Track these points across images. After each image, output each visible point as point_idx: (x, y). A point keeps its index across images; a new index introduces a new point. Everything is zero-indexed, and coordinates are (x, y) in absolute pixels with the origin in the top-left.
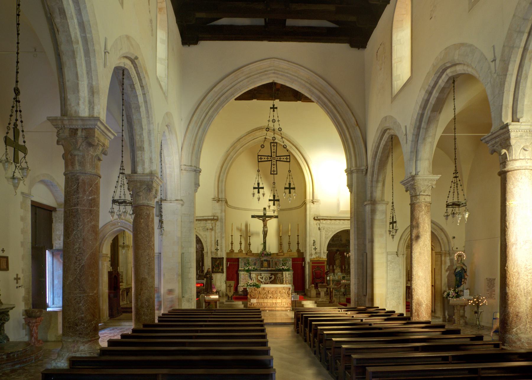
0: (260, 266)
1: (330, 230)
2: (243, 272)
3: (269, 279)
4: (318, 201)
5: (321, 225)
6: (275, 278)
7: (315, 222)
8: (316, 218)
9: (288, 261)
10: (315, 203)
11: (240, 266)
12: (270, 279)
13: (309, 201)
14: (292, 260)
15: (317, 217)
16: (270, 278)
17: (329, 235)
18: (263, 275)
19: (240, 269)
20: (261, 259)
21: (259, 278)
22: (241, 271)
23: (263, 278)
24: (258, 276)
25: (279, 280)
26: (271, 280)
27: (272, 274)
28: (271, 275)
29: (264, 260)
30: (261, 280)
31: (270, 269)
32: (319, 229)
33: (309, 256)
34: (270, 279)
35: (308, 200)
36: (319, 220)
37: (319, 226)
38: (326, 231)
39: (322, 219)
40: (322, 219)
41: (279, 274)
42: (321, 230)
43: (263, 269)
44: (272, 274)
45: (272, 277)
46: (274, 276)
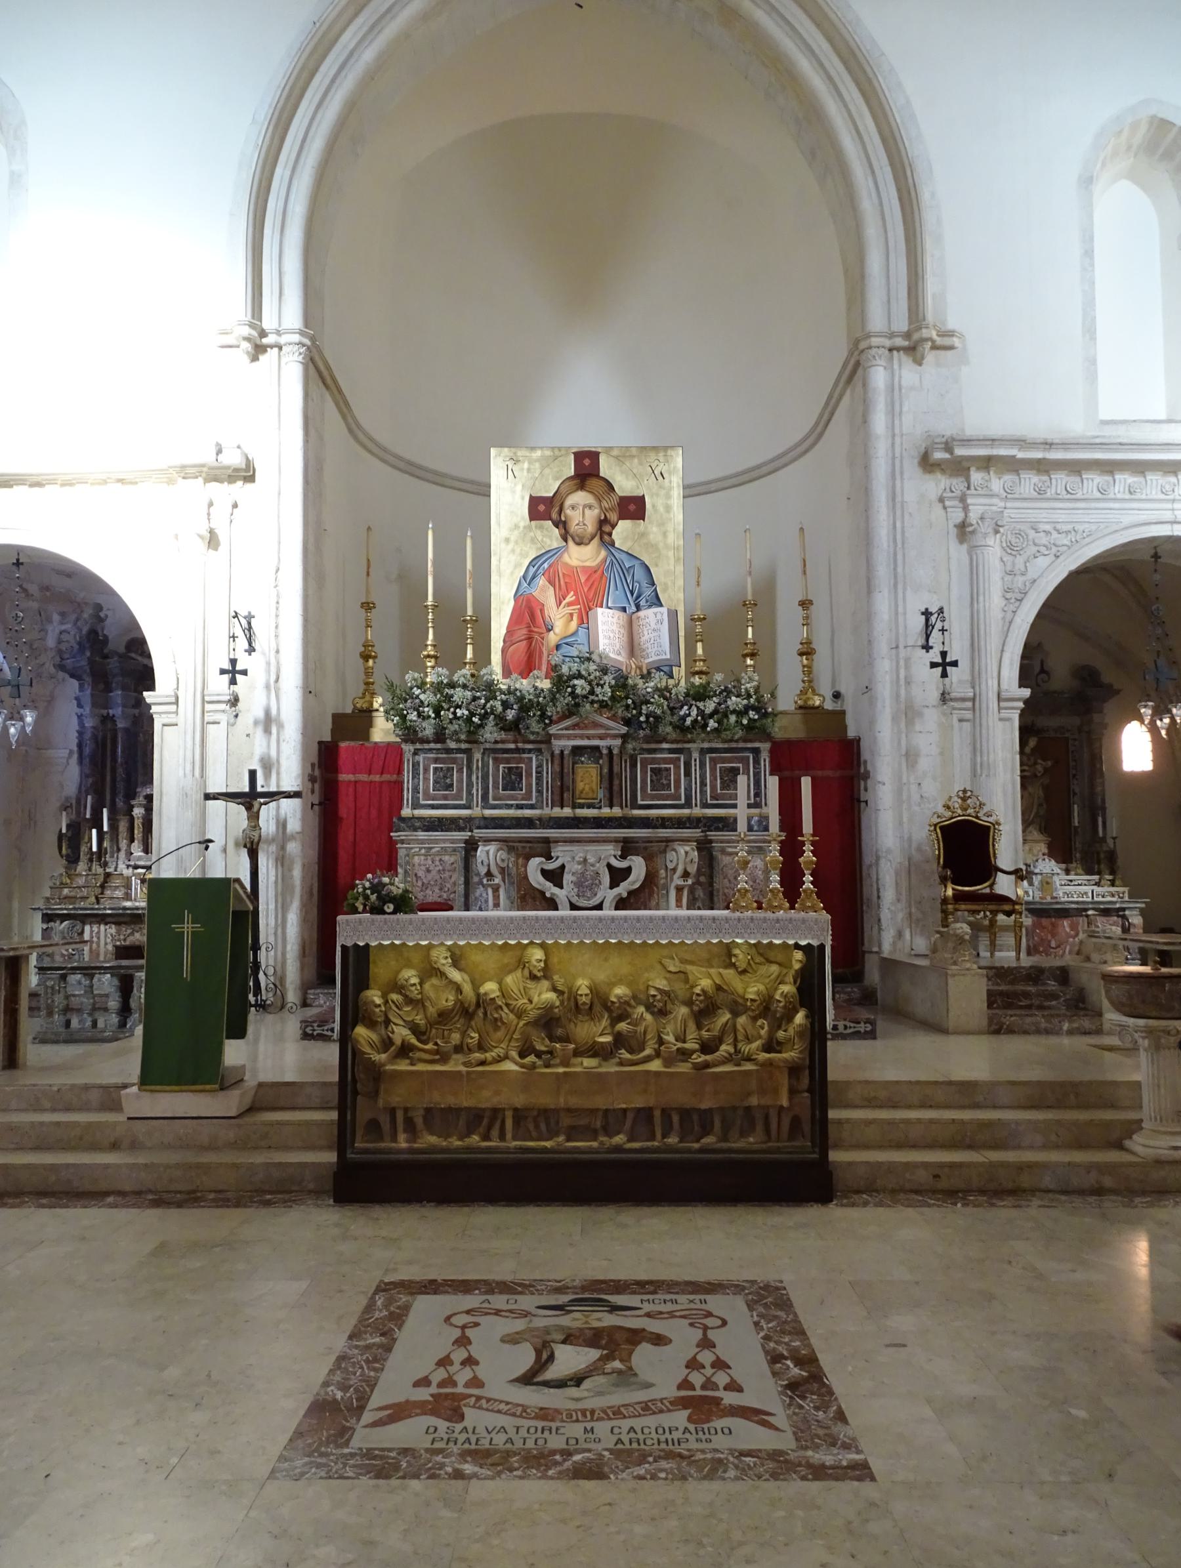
0: (547, 795)
1: (1043, 539)
2: (422, 835)
3: (606, 879)
4: (946, 341)
5: (977, 506)
6: (650, 879)
7: (936, 484)
8: (939, 455)
9: (745, 761)
10: (930, 357)
11: (407, 795)
12: (614, 884)
13: (888, 343)
14: (772, 752)
15: (948, 448)
16: (618, 876)
17: (1032, 574)
18: (563, 855)
19: (406, 812)
20: (558, 744)
21: (536, 879)
22: (413, 824)
23: (568, 878)
24: (528, 858)
25: (679, 889)
26: (623, 889)
27: (628, 848)
28: (623, 857)
29: (577, 750)
30: (550, 889)
31: (617, 811)
32: (963, 531)
33: (895, 719)
34: (614, 884)
35: (879, 335)
36: (959, 468)
37: (957, 516)
38: (1010, 549)
39: (987, 463)
40: (987, 463)
41: (682, 849)
42: (978, 540)
43: (567, 812)
44: (628, 848)
45: (628, 870)
46: (649, 859)
